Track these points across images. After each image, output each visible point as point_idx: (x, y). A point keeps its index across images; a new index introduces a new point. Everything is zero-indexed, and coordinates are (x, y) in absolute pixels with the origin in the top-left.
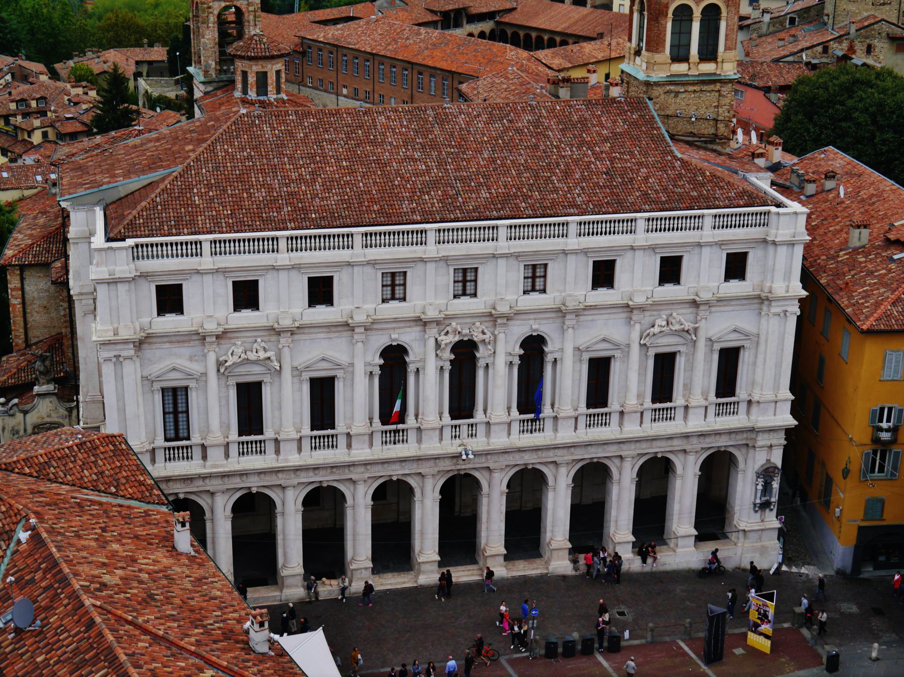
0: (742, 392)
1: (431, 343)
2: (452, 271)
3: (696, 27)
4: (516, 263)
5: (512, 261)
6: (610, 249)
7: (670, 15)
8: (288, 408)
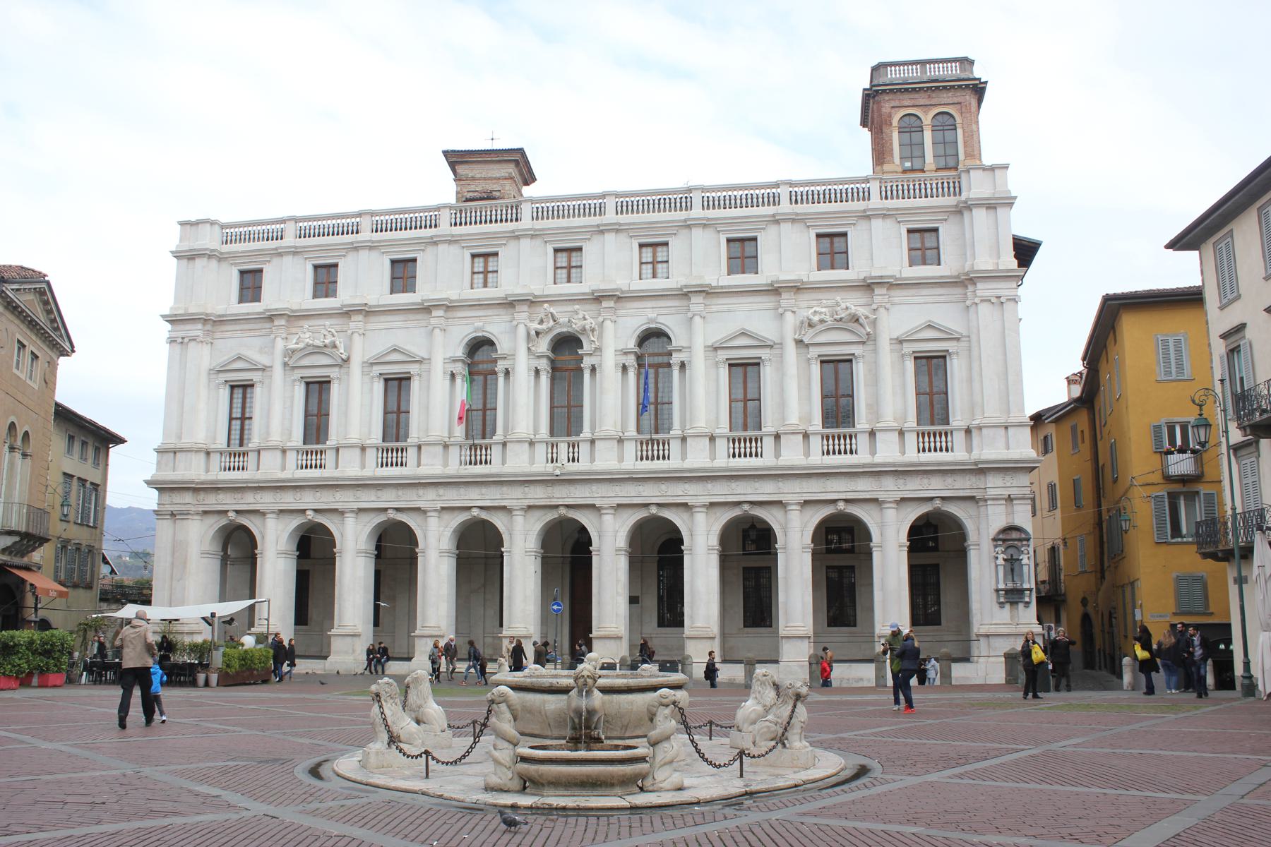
0: (958, 418)
1: (522, 331)
2: (551, 252)
3: (928, 136)
4: (628, 240)
5: (623, 237)
6: (746, 220)
7: (895, 122)
8: (357, 410)
